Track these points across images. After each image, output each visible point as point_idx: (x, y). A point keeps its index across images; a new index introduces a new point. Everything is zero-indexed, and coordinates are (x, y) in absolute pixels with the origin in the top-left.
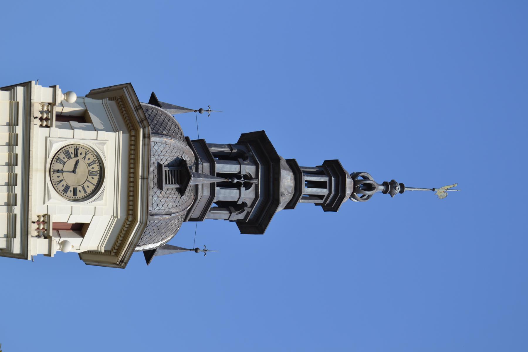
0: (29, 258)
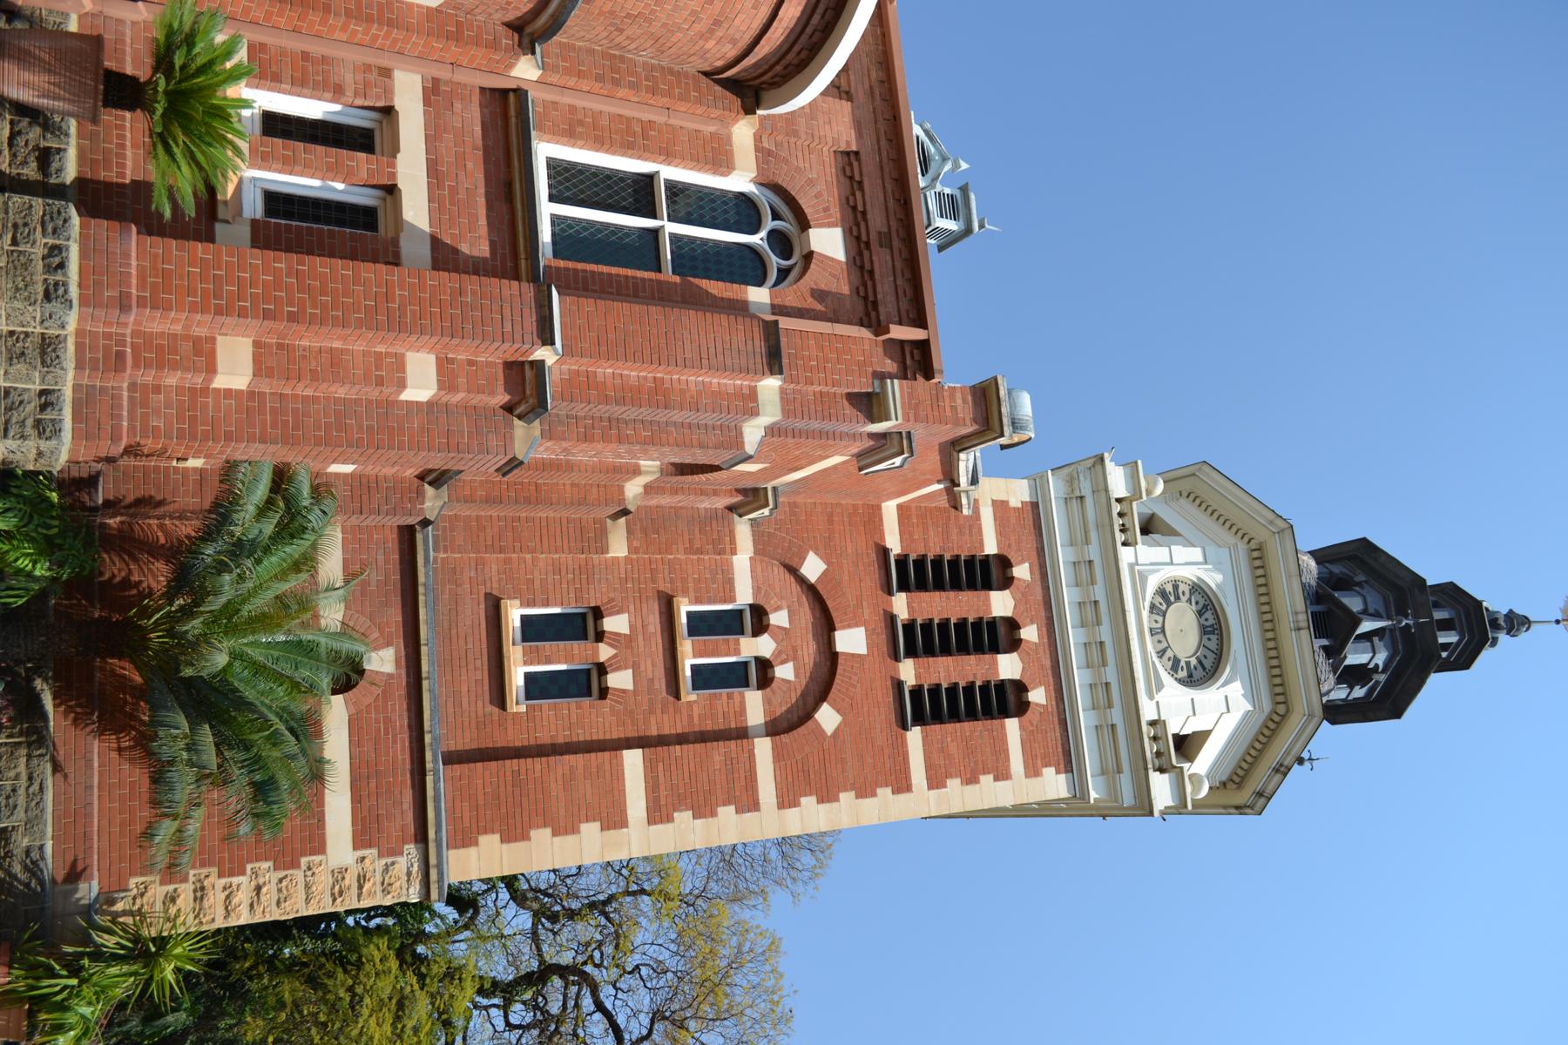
0: (1156, 813)
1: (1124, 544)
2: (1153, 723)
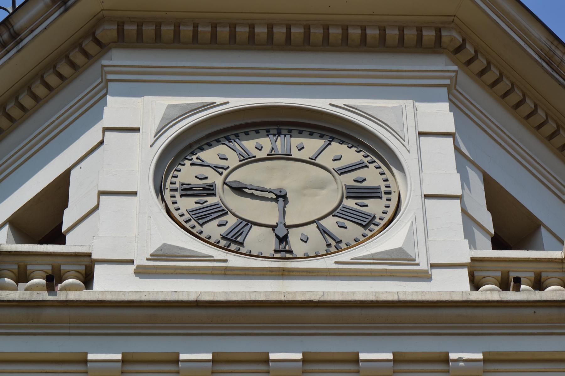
1: (88, 280)
2: (475, 285)
